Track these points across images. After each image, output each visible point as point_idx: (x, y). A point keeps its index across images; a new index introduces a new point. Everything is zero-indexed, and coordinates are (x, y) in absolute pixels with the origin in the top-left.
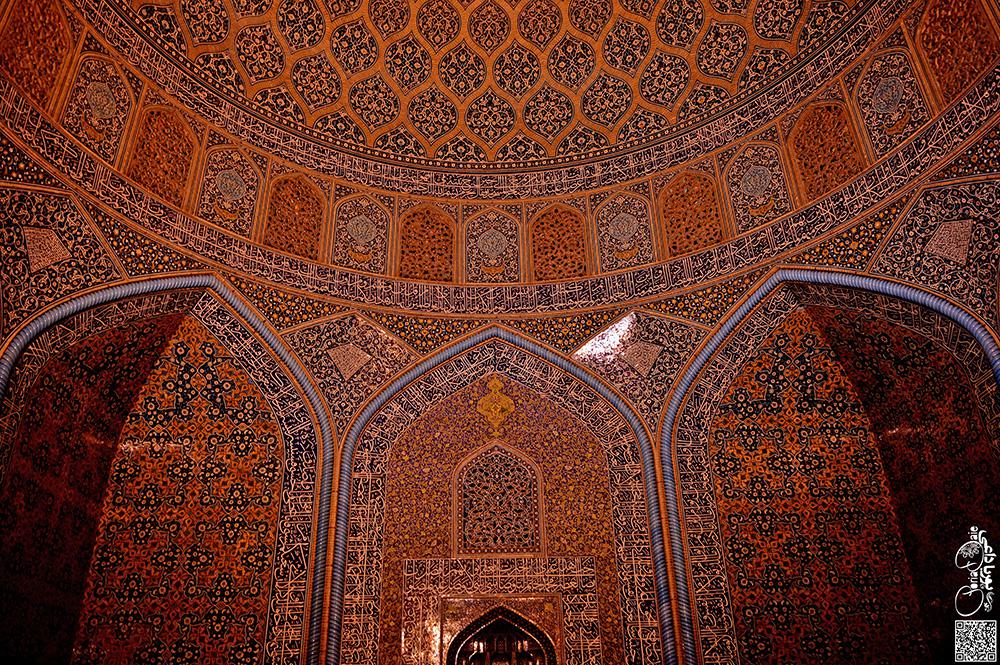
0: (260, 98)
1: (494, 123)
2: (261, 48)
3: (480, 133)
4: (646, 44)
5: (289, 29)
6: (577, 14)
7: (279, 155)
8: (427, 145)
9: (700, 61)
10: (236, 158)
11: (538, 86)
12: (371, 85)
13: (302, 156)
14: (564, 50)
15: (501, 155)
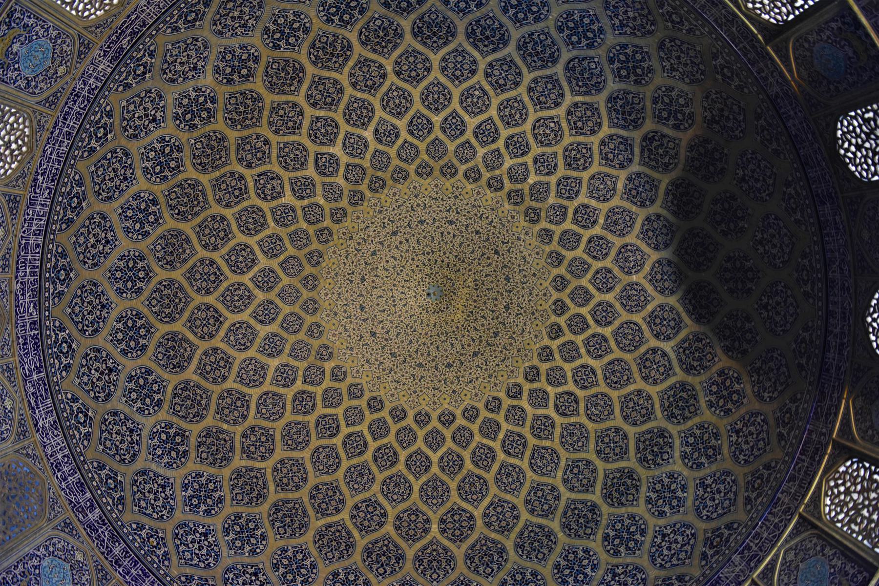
0: (108, 108)
1: (95, 380)
2: (147, 116)
3: (83, 366)
4: (213, 512)
5: (158, 146)
6: (208, 435)
7: (56, 124)
8: (61, 306)
9: (228, 570)
10: (61, 70)
11: (138, 418)
12: (110, 236)
13: (51, 154)
14: (176, 434)
15: (69, 396)
